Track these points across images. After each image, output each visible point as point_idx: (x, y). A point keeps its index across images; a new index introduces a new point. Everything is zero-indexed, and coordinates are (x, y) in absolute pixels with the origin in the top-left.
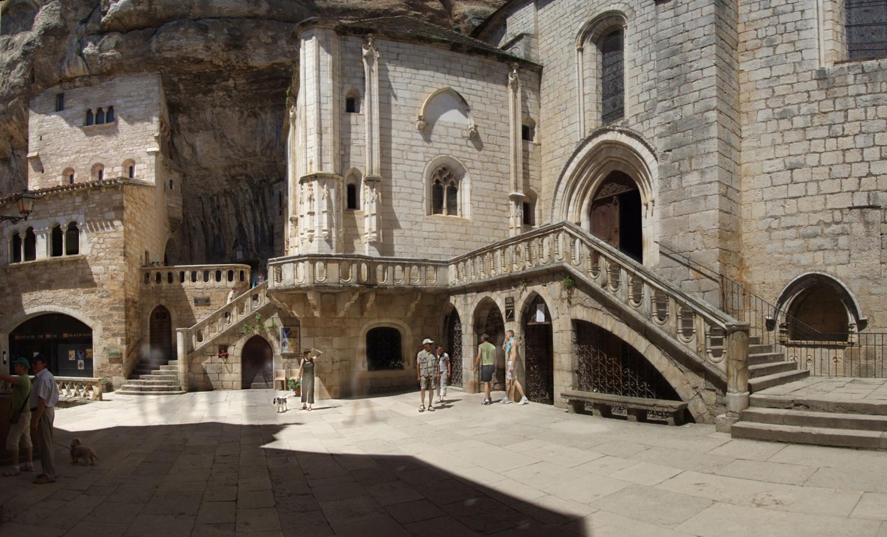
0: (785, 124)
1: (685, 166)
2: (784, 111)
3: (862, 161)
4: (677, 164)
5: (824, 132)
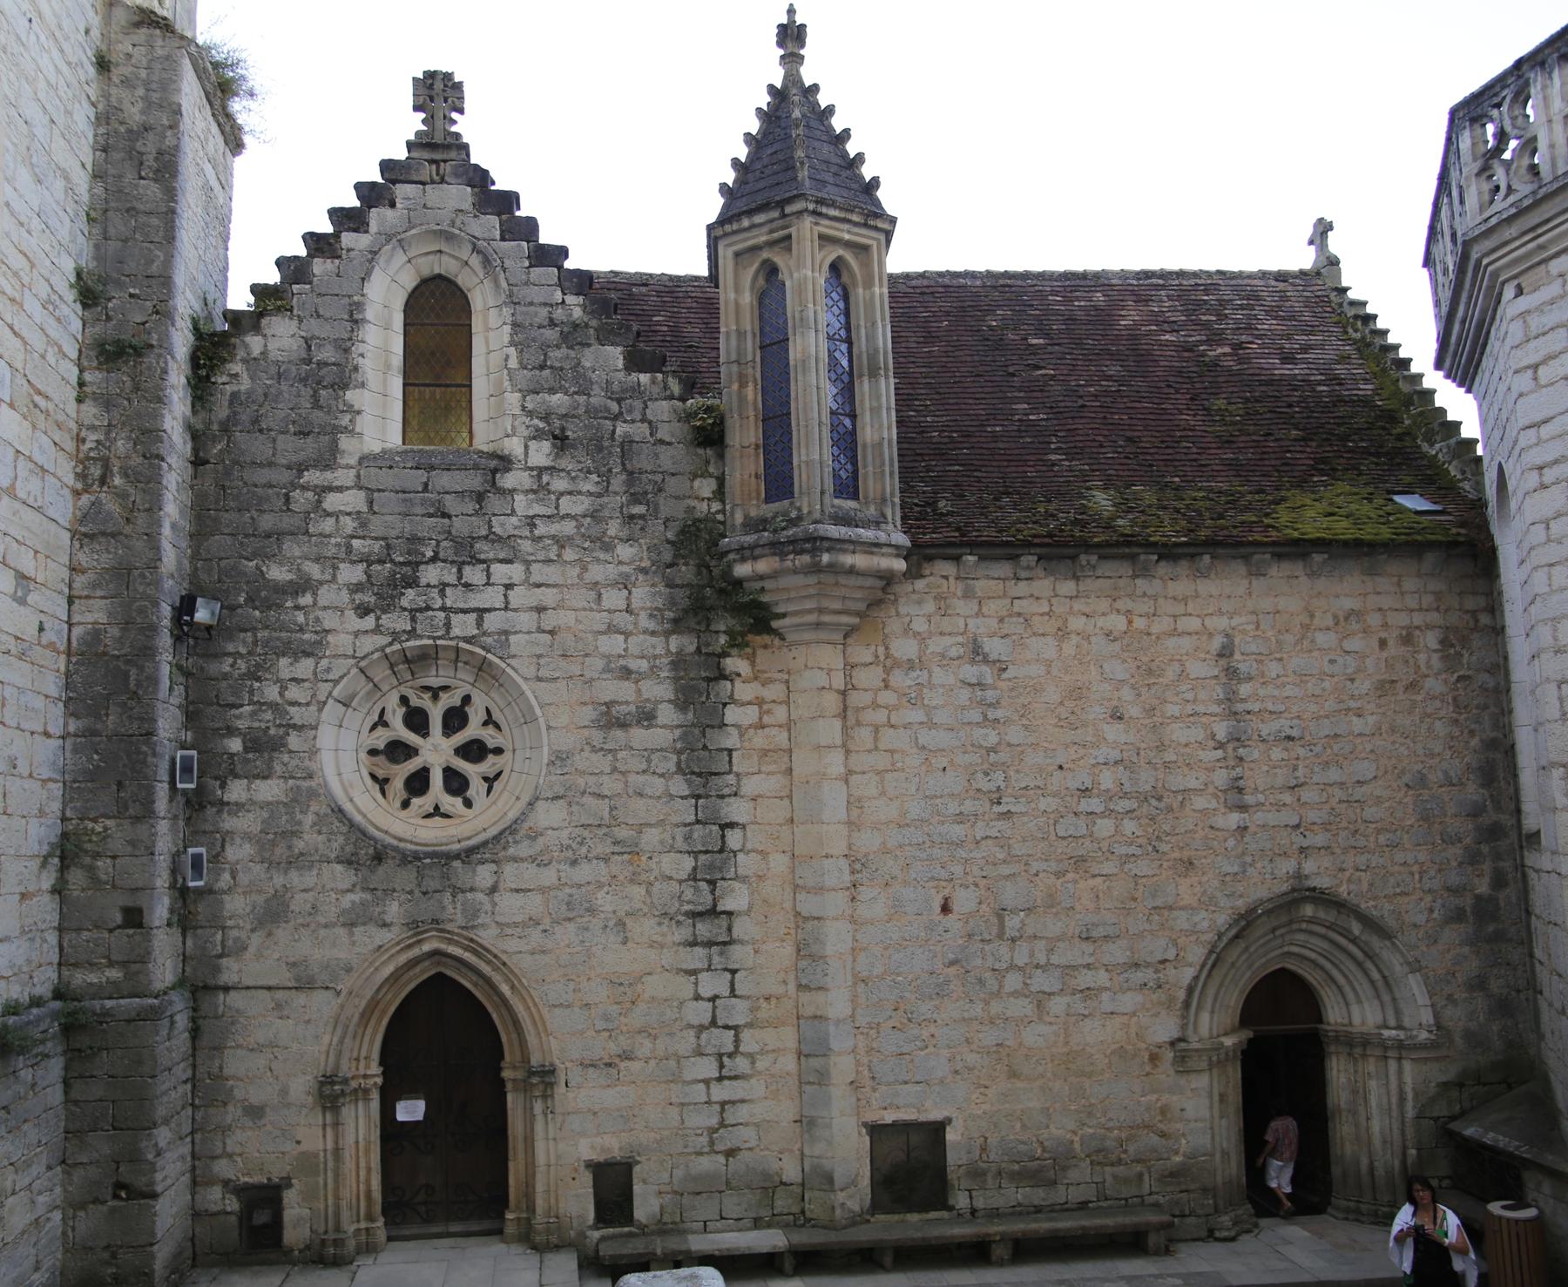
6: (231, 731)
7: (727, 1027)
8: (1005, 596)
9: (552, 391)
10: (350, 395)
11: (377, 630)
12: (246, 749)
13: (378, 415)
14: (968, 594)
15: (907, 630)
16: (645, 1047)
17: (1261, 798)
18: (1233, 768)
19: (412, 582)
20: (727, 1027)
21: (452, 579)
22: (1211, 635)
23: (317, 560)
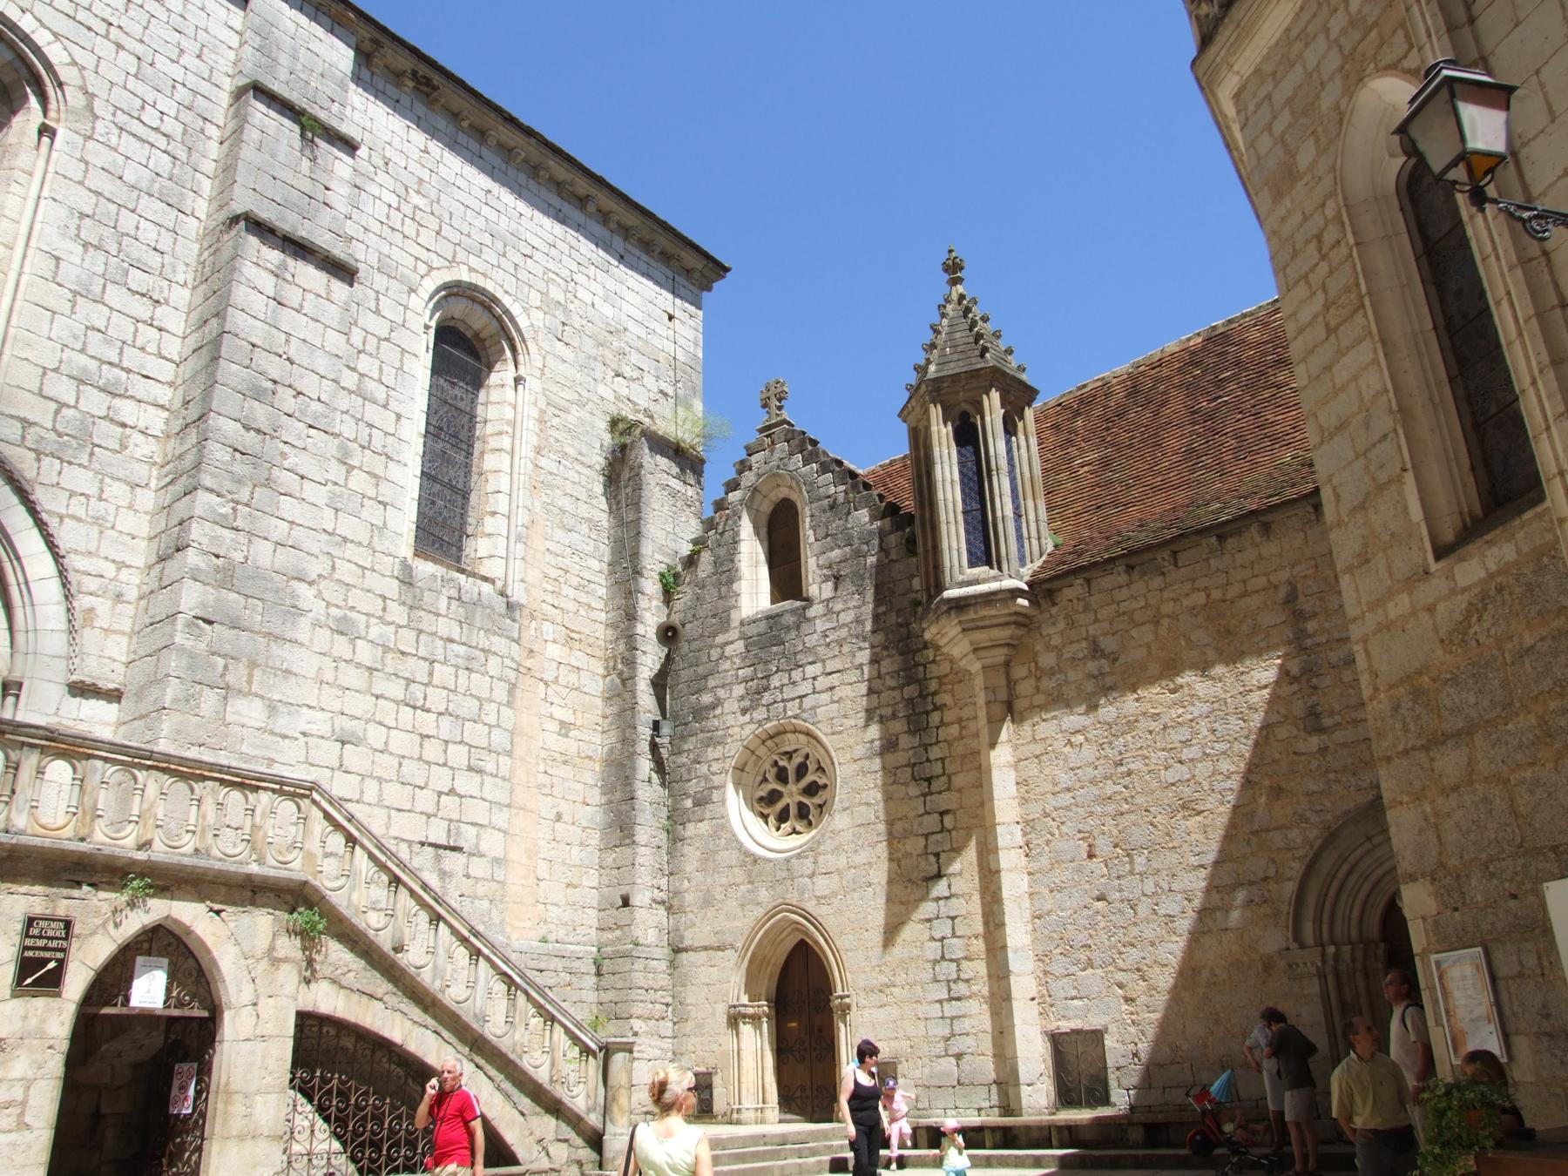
0: (341, 646)
2: (345, 618)
3: (445, 765)
4: (221, 662)
5: (396, 690)
6: (687, 795)
7: (951, 960)
8: (1113, 601)
9: (832, 549)
10: (735, 586)
11: (751, 722)
12: (695, 805)
13: (754, 591)
14: (1087, 609)
15: (1049, 647)
16: (901, 978)
17: (1338, 718)
18: (1310, 696)
19: (766, 689)
20: (951, 960)
21: (786, 681)
22: (1276, 588)
23: (723, 686)
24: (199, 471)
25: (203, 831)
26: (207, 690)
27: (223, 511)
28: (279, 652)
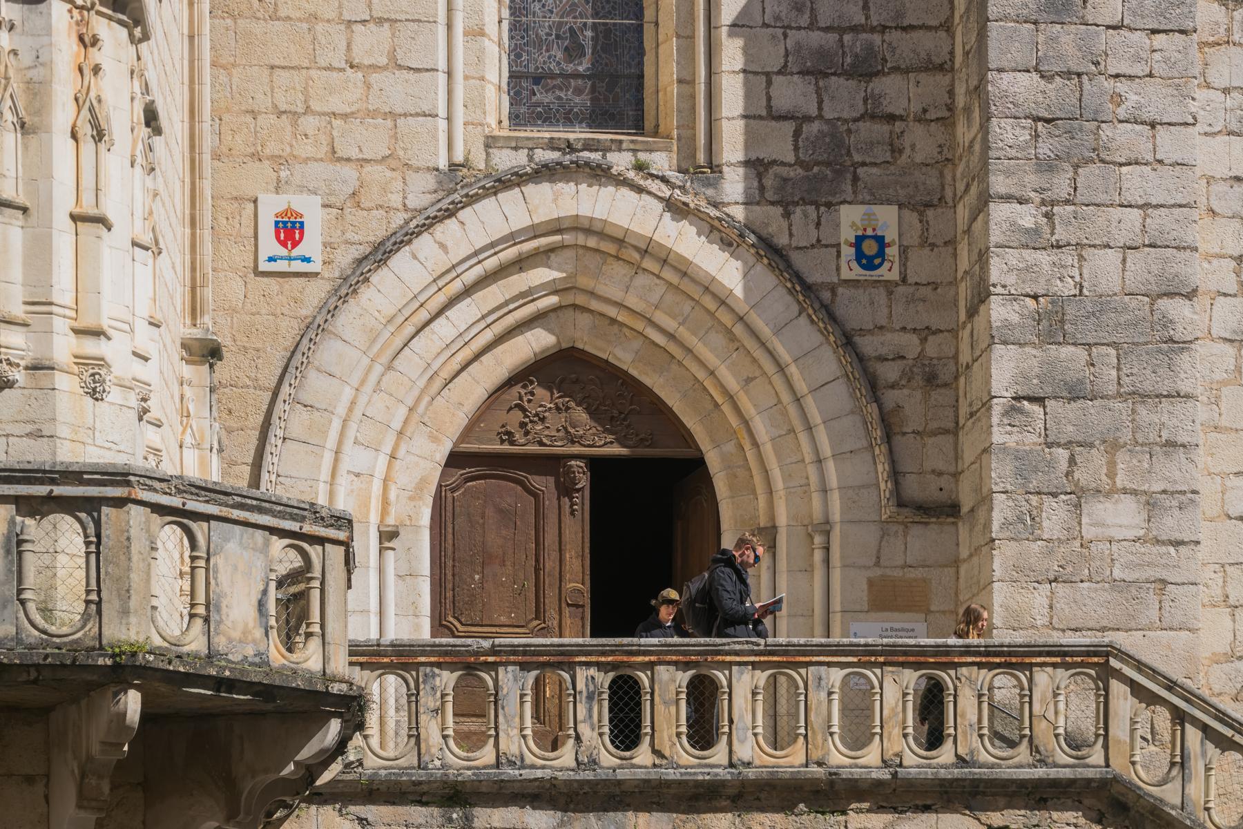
1: (1092, 468)
4: (1062, 454)
24: (987, 173)
25: (965, 733)
26: (1048, 501)
27: (1028, 222)
28: (1155, 418)
